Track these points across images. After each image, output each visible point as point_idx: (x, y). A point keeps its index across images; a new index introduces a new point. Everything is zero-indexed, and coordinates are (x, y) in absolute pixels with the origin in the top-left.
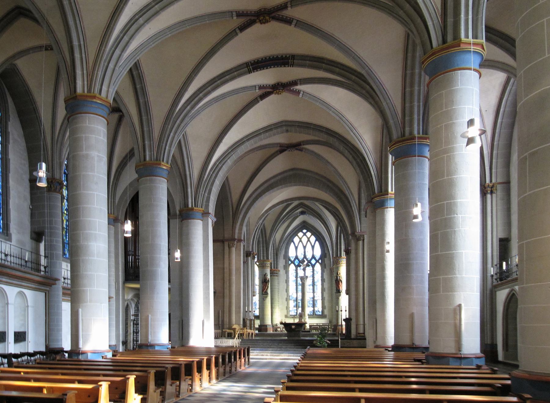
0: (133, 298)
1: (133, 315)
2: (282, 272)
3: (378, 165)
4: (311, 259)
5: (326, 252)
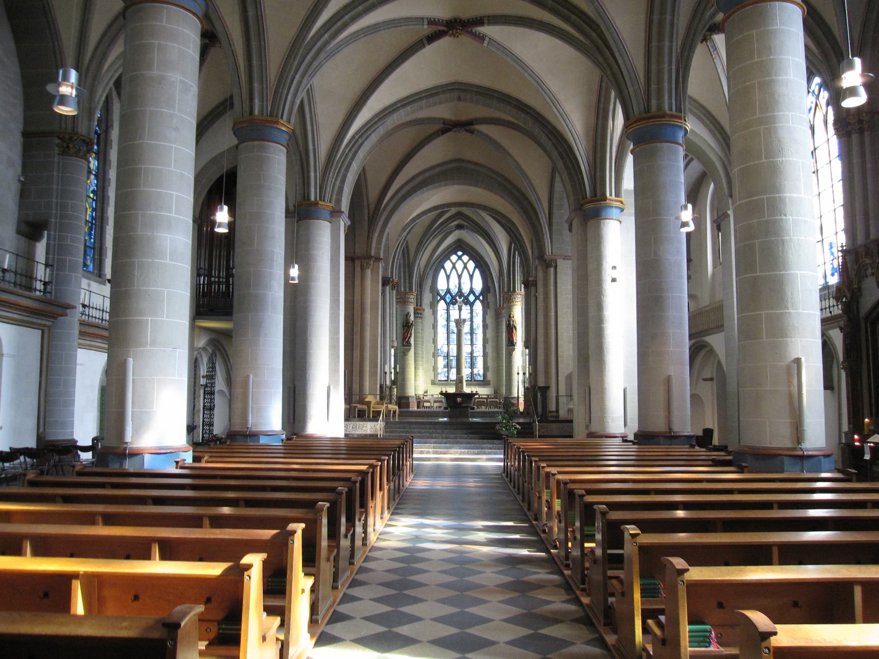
0: (206, 347)
1: (203, 377)
2: (427, 312)
3: (591, 158)
4: (469, 295)
5: (490, 284)
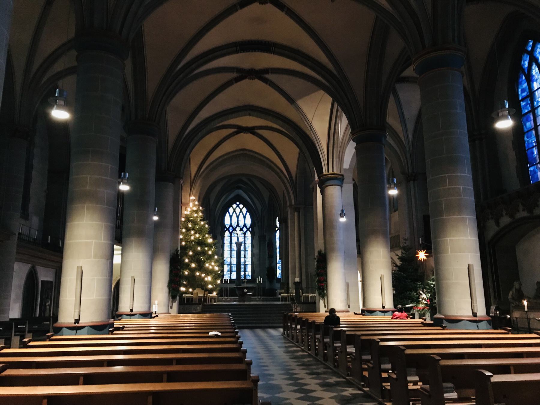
4: (243, 228)
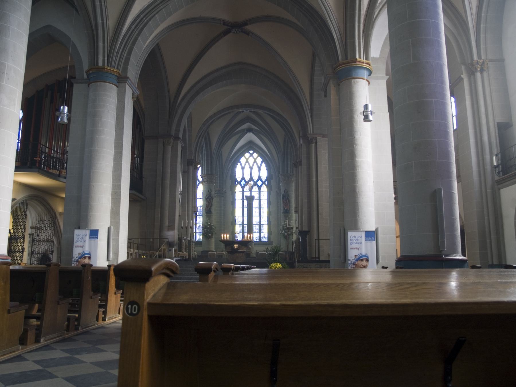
4: (258, 181)
